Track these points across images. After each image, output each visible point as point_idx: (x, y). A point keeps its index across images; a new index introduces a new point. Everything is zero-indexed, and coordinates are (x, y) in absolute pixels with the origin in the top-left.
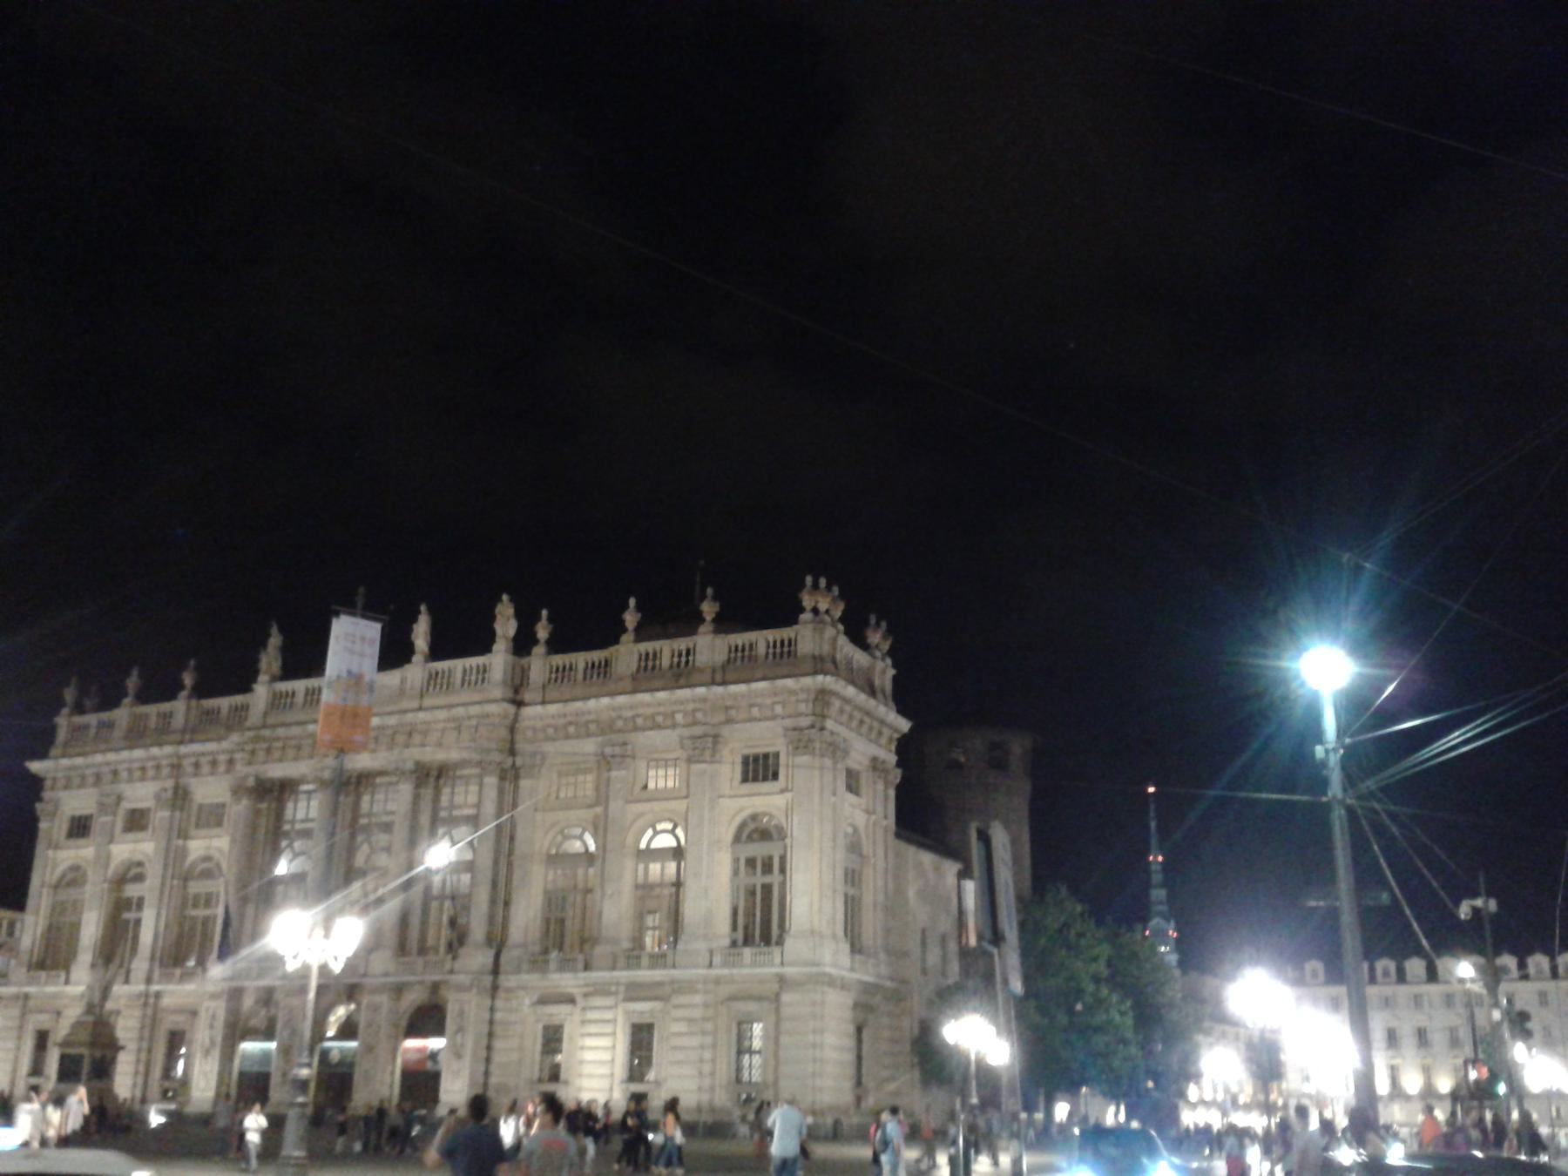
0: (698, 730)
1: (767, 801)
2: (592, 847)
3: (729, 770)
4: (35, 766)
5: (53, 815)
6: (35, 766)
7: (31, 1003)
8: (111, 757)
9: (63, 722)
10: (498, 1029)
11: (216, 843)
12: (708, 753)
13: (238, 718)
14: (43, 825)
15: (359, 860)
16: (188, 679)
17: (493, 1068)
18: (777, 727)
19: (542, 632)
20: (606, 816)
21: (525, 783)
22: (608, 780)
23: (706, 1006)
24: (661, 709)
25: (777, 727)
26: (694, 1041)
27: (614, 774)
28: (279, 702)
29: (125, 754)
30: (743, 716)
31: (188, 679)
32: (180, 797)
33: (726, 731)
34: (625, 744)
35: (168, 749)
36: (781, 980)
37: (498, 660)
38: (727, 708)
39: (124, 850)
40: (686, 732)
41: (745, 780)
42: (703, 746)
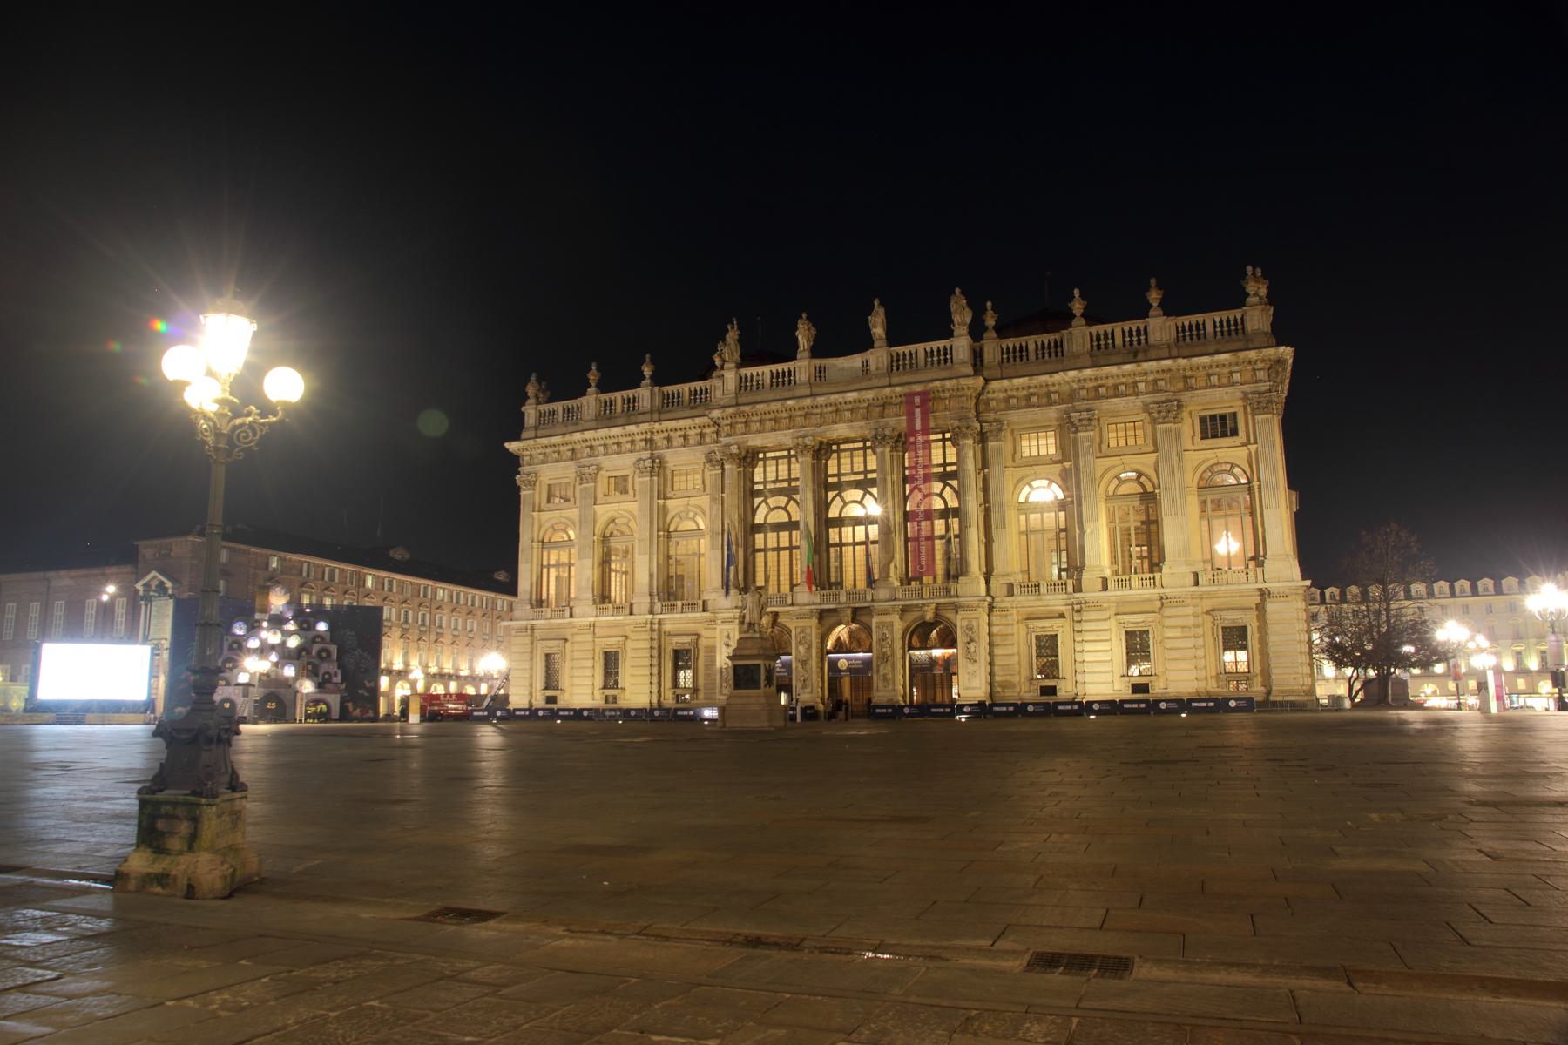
0: (1160, 397)
1: (1231, 451)
2: (702, 526)
3: (1188, 427)
4: (512, 446)
5: (532, 485)
6: (512, 446)
7: (537, 633)
8: (589, 435)
9: (530, 412)
10: (997, 640)
14: (525, 493)
15: (833, 513)
17: (996, 669)
19: (990, 321)
20: (1077, 470)
22: (1075, 441)
23: (1196, 616)
26: (1190, 643)
28: (743, 384)
29: (602, 432)
30: (1202, 383)
32: (657, 467)
33: (1185, 397)
34: (1088, 410)
35: (645, 427)
38: (1185, 378)
40: (1148, 398)
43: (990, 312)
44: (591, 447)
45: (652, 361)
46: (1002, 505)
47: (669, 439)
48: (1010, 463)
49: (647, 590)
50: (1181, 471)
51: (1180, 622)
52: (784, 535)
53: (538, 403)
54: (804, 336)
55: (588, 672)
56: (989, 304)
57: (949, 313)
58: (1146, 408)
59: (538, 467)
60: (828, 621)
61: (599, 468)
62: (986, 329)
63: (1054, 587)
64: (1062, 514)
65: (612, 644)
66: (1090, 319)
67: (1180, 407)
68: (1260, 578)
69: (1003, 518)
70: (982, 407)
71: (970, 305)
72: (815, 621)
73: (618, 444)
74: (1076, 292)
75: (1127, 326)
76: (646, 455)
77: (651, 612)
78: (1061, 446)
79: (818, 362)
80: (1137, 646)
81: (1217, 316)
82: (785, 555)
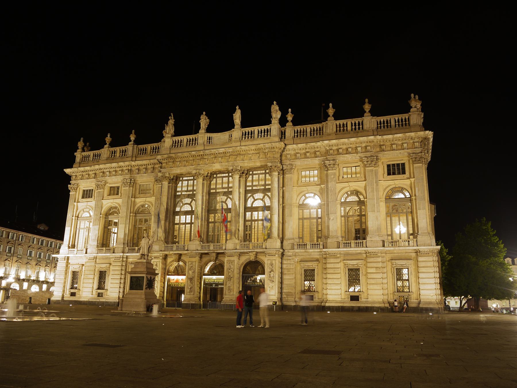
0: (368, 154)
3: (382, 170)
4: (67, 171)
6: (67, 171)
8: (102, 166)
9: (78, 155)
10: (285, 271)
11: (148, 199)
12: (373, 163)
13: (156, 151)
16: (133, 137)
17: (284, 286)
18: (405, 153)
19: (290, 117)
20: (327, 189)
21: (287, 176)
22: (327, 175)
24: (351, 146)
25: (405, 153)
27: (329, 171)
28: (175, 144)
29: (108, 165)
31: (133, 137)
32: (132, 183)
33: (380, 155)
34: (334, 160)
35: (127, 163)
36: (417, 252)
37: (275, 127)
38: (380, 146)
39: (108, 203)
40: (362, 155)
41: (389, 174)
42: (372, 160)
43: (290, 114)
44: (103, 172)
45: (135, 134)
46: (291, 205)
47: (139, 169)
48: (296, 184)
49: (122, 241)
50: (377, 190)
51: (375, 265)
52: (189, 217)
53: (83, 151)
54: (204, 122)
55: (91, 281)
56: (290, 110)
57: (270, 112)
58: (361, 160)
59: (79, 181)
60: (205, 259)
61: (106, 183)
62: (288, 121)
63: (313, 246)
64: (319, 210)
65: (103, 267)
66: (337, 117)
67: (377, 159)
68: (415, 244)
69: (291, 211)
70: (283, 158)
71: (280, 109)
72: (197, 258)
73: (116, 171)
74: (331, 105)
75: (353, 121)
76: (128, 177)
77: (123, 252)
78: (321, 178)
79: (209, 135)
80: (354, 277)
81: (397, 117)
82: (188, 226)
